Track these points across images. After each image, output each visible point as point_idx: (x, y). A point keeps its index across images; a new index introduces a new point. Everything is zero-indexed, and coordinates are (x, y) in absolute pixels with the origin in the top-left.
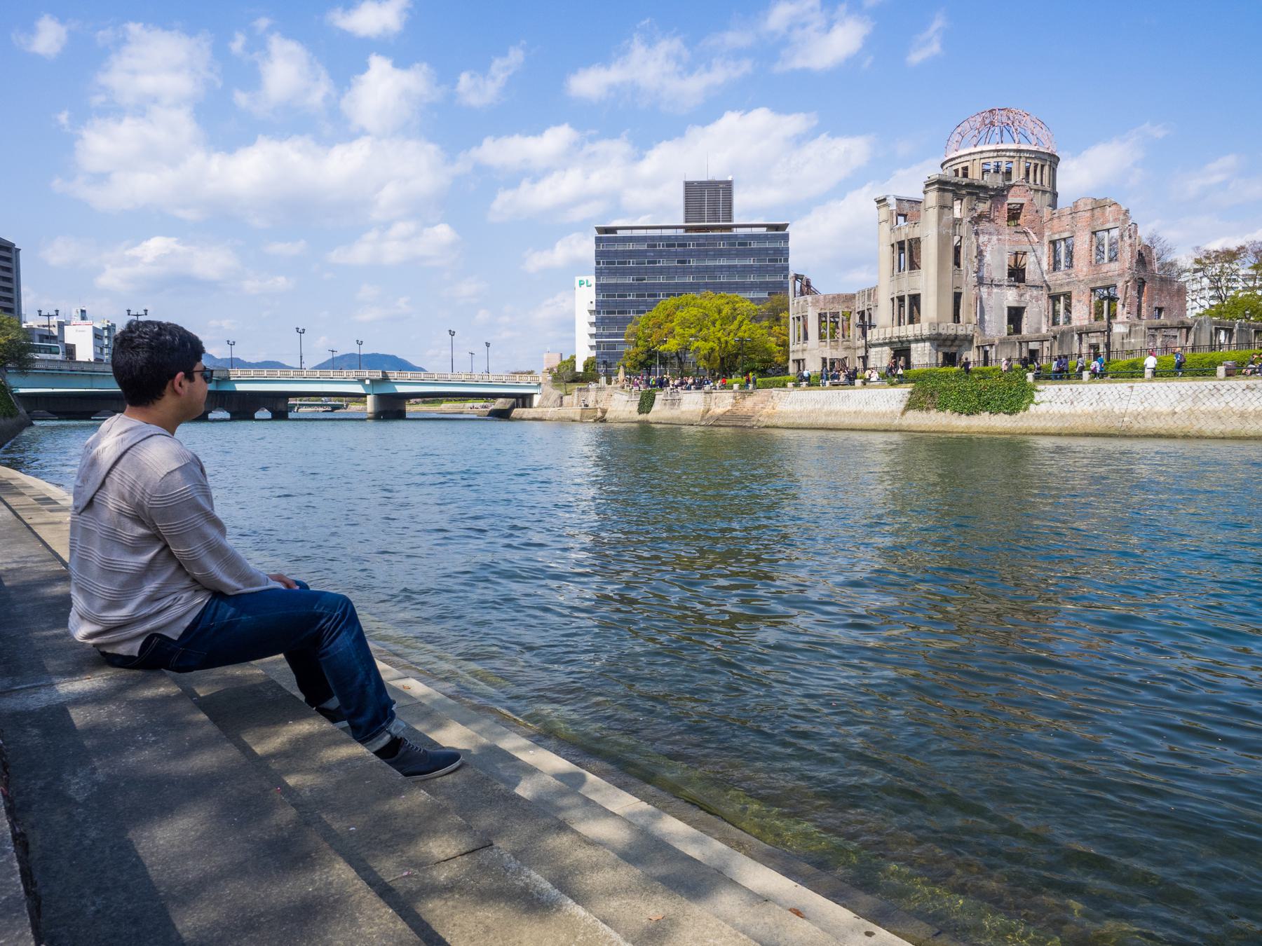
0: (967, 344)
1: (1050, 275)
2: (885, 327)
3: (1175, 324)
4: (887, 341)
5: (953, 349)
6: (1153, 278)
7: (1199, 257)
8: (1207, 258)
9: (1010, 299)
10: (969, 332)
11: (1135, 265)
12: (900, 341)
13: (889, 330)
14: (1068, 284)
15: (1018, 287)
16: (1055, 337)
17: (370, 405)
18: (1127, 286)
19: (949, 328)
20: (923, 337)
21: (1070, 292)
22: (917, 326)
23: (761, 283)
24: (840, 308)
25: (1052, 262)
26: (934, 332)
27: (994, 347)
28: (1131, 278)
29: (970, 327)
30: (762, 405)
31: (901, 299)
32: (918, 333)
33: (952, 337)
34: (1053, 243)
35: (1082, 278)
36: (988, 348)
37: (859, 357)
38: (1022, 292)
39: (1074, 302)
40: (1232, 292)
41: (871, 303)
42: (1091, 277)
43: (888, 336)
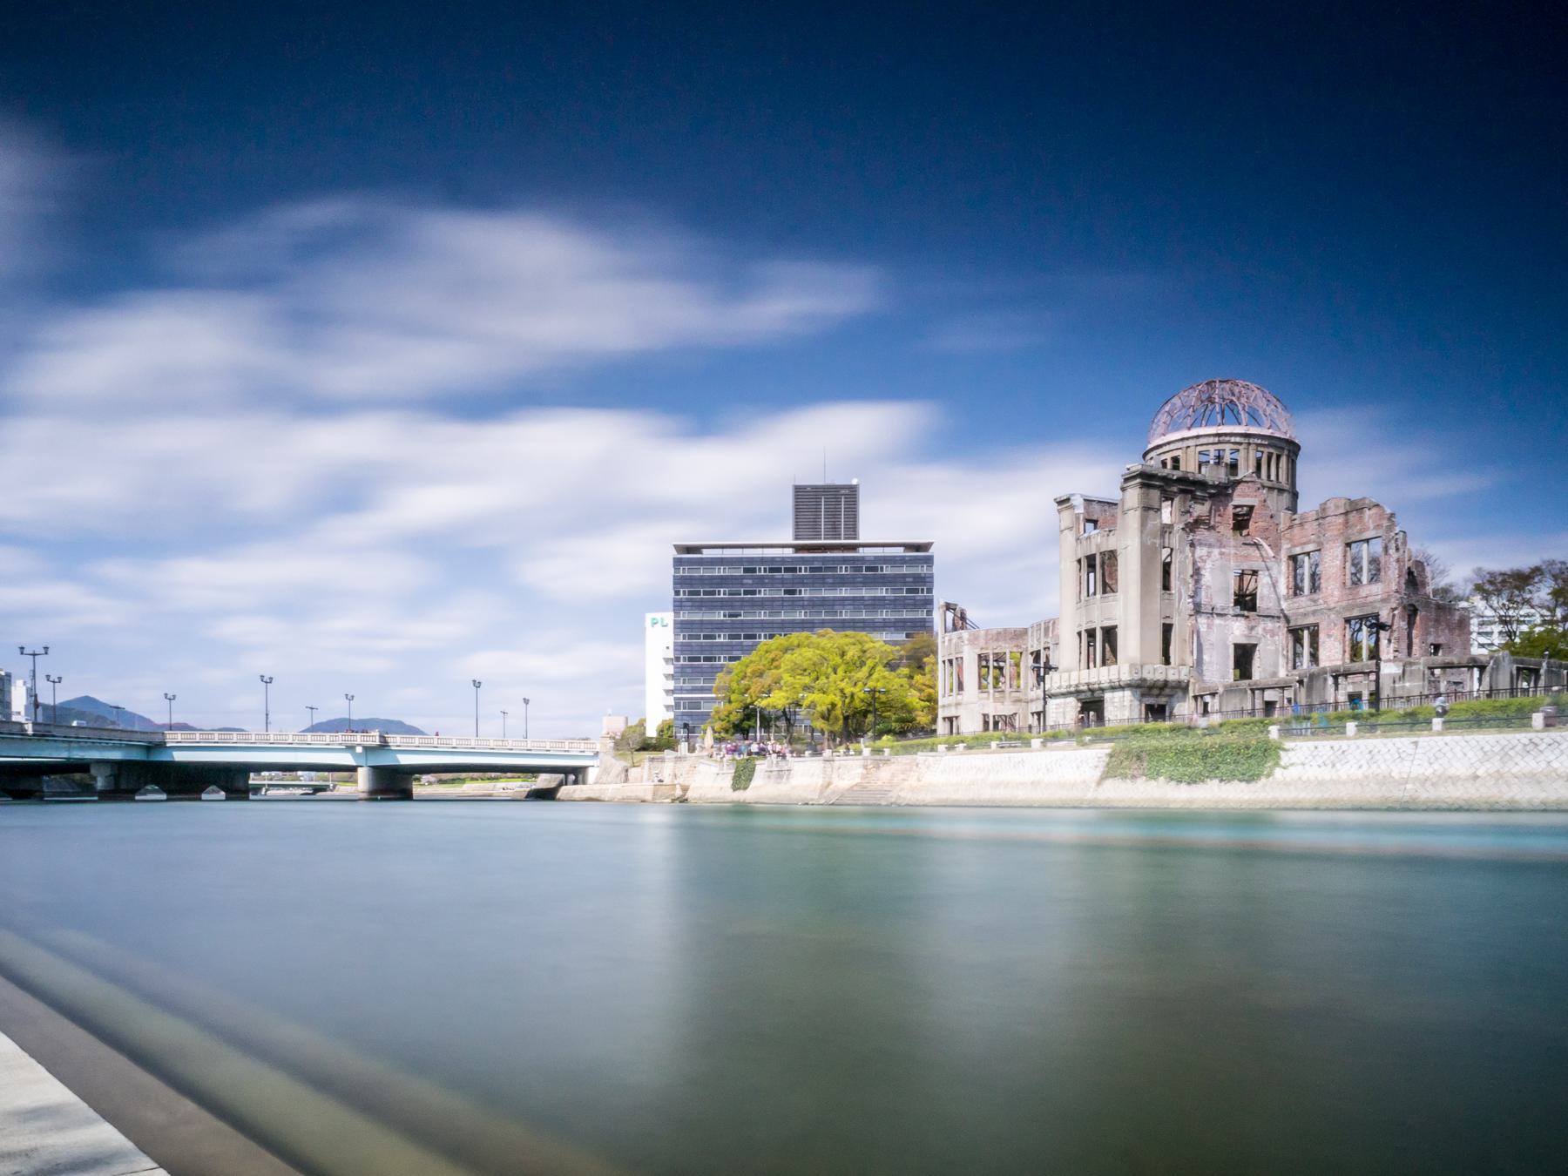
0: (1180, 694)
1: (1289, 602)
2: (1069, 671)
3: (1464, 662)
4: (1072, 689)
5: (1162, 700)
6: (1427, 604)
7: (1480, 582)
8: (1491, 583)
9: (1237, 633)
10: (1184, 678)
11: (1404, 586)
12: (1090, 690)
13: (1074, 675)
14: (1314, 613)
15: (1247, 617)
16: (1301, 682)
17: (363, 781)
18: (1394, 615)
19: (1156, 672)
20: (1122, 684)
21: (1317, 625)
22: (1114, 668)
23: (897, 621)
24: (1006, 647)
25: (1292, 584)
26: (1137, 677)
27: (1217, 696)
28: (1399, 604)
29: (1185, 670)
30: (902, 777)
31: (1091, 634)
32: (1114, 677)
33: (1159, 684)
34: (1293, 558)
35: (1332, 605)
36: (1208, 699)
37: (1033, 714)
38: (1253, 623)
39: (1322, 637)
40: (1525, 628)
41: (1049, 640)
42: (1344, 603)
43: (1074, 682)
